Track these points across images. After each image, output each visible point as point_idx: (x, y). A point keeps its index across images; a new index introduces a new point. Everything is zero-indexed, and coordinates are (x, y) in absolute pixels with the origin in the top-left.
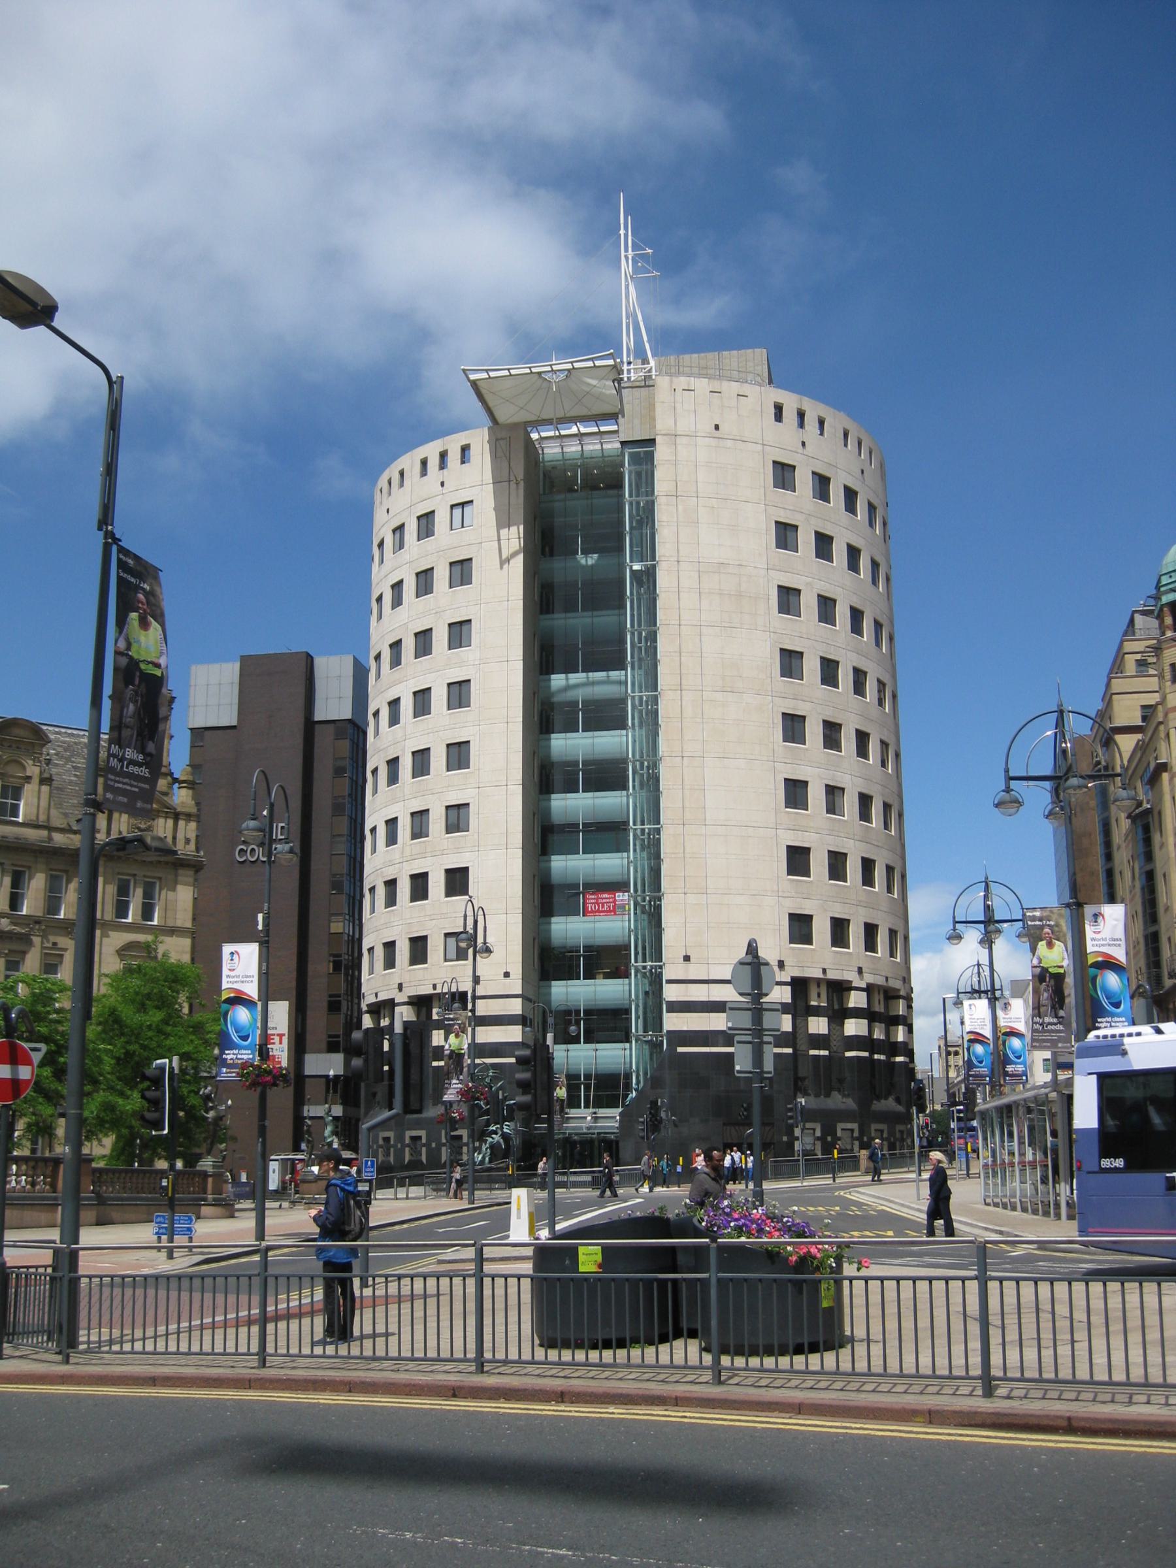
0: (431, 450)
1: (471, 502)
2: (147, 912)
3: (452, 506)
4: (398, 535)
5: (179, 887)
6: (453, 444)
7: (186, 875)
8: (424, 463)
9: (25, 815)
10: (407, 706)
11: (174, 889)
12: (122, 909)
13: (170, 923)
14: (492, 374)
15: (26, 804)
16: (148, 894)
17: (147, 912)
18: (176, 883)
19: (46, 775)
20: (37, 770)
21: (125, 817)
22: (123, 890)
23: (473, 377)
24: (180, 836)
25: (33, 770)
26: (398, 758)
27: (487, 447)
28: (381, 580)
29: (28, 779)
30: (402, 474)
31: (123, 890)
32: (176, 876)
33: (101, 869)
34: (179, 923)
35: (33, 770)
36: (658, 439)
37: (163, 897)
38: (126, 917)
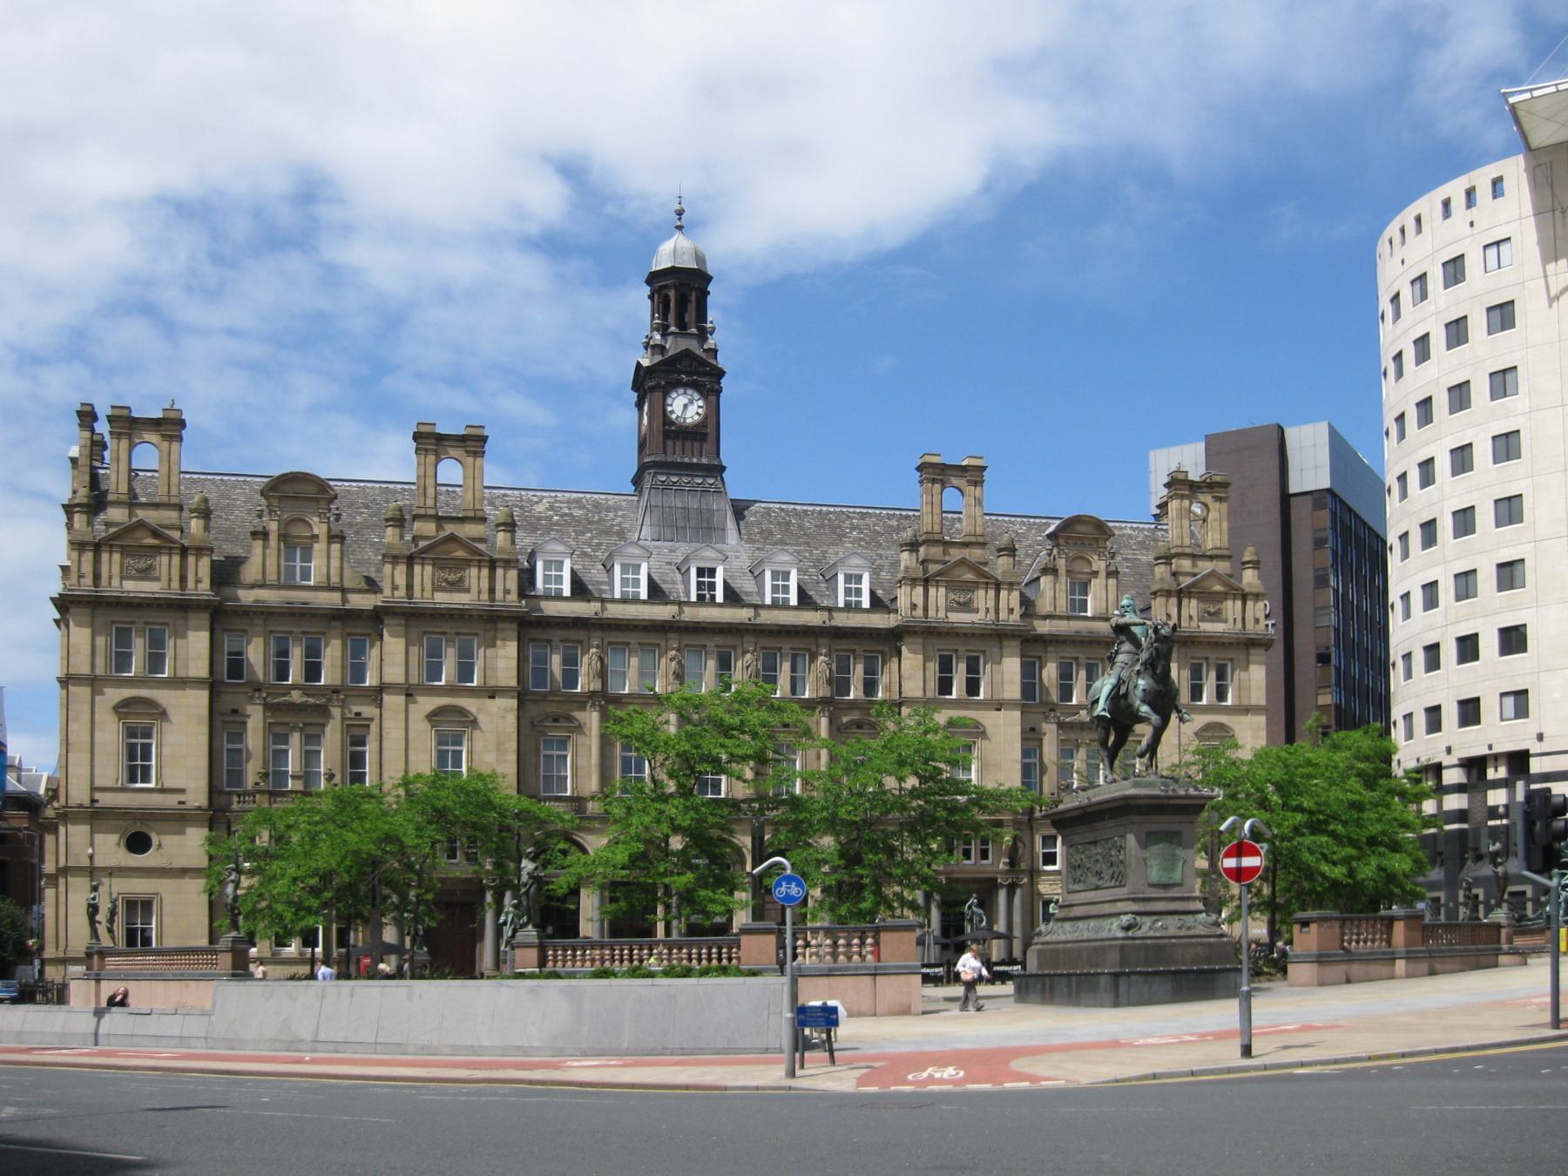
0: (1455, 189)
1: (1509, 239)
2: (1221, 694)
3: (1486, 247)
4: (1418, 285)
5: (1252, 667)
6: (1481, 178)
7: (1256, 654)
8: (1446, 204)
9: (1095, 609)
11: (1247, 669)
12: (1196, 693)
13: (1245, 702)
14: (1536, 93)
15: (1095, 598)
16: (1221, 676)
17: (1221, 694)
18: (1248, 663)
19: (1112, 568)
20: (1102, 564)
21: (1194, 602)
22: (1196, 674)
23: (1512, 100)
24: (1249, 615)
25: (1099, 564)
26: (1434, 520)
27: (1524, 176)
29: (1095, 574)
30: (1418, 220)
31: (1196, 674)
32: (1248, 655)
33: (1174, 655)
34: (1253, 702)
35: (1099, 564)
37: (1236, 679)
38: (1200, 699)
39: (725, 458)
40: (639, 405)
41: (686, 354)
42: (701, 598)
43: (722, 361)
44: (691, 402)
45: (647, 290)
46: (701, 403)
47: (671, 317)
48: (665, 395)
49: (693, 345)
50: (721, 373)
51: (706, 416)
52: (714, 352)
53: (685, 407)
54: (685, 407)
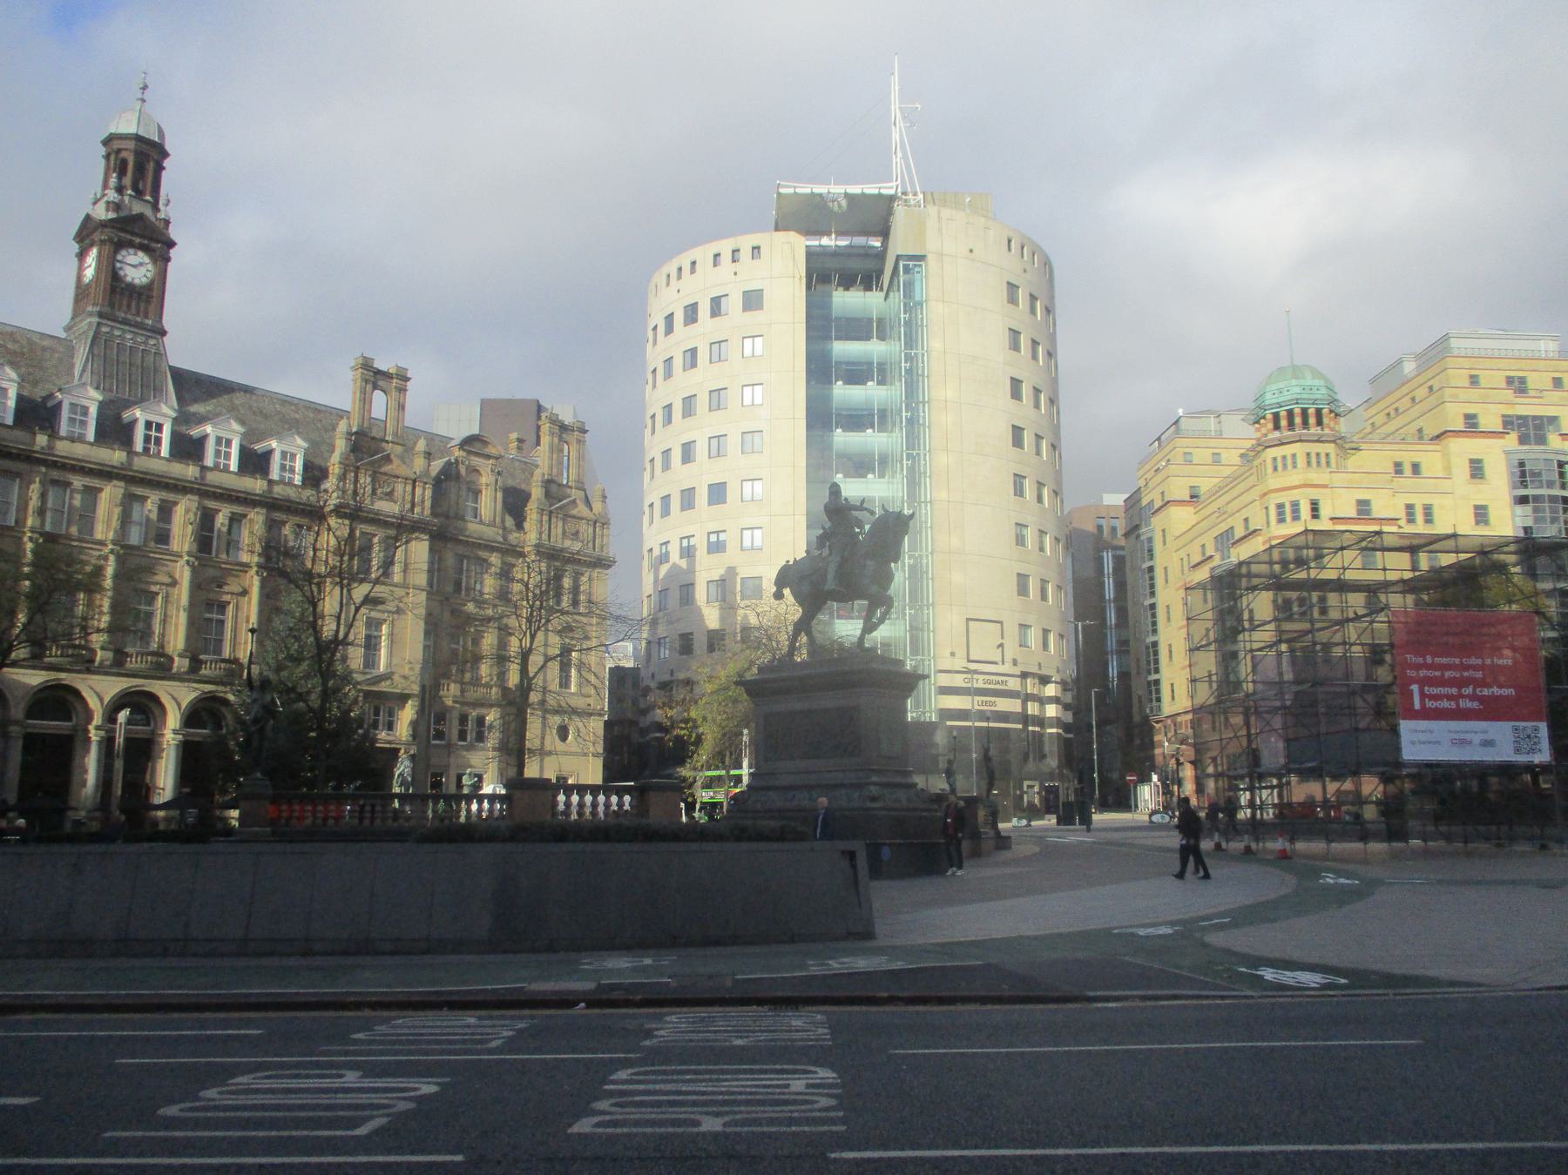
10: (676, 455)
28: (654, 358)
36: (930, 257)
39: (168, 321)
40: (81, 256)
41: (141, 217)
42: (146, 450)
43: (173, 233)
44: (141, 264)
45: (103, 151)
46: (150, 267)
47: (127, 180)
48: (116, 252)
49: (148, 212)
50: (171, 244)
51: (152, 282)
52: (167, 222)
53: (136, 268)
54: (136, 268)
